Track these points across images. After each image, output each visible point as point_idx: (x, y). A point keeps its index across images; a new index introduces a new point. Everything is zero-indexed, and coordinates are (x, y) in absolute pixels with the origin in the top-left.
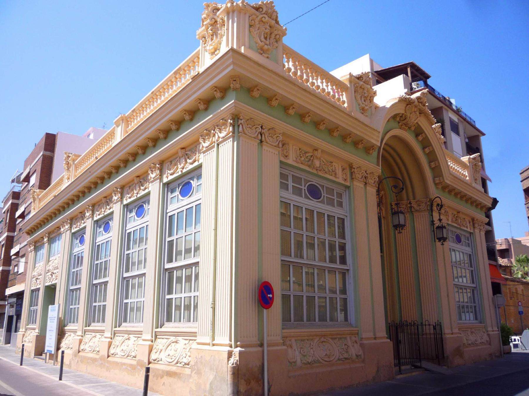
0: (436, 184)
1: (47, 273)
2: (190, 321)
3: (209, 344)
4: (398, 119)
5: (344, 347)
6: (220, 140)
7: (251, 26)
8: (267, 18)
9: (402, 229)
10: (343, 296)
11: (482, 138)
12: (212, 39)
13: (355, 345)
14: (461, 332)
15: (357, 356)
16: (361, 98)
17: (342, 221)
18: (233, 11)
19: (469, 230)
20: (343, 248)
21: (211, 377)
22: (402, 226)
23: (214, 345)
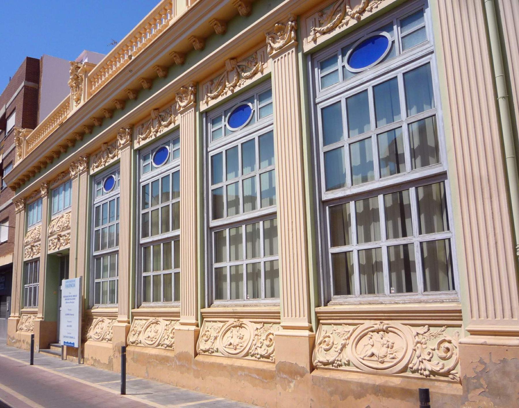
1: (49, 237)
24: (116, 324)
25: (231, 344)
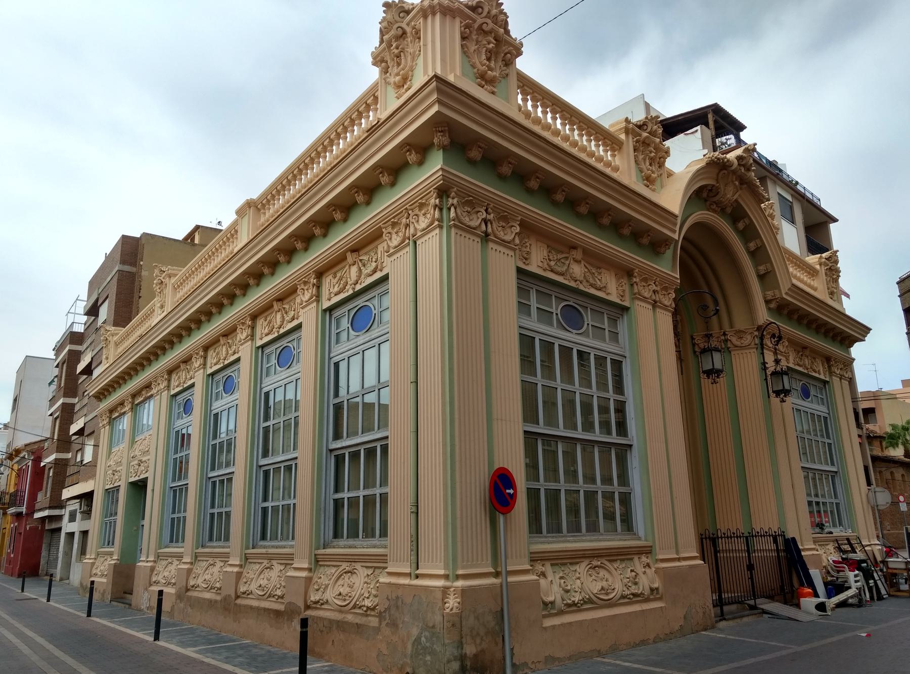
0: (767, 302)
2: (373, 536)
3: (409, 575)
4: (705, 195)
5: (629, 574)
6: (419, 234)
7: (463, 38)
8: (491, 25)
9: (718, 377)
10: (623, 489)
11: (832, 226)
12: (399, 64)
13: (648, 570)
14: (818, 547)
15: (652, 590)
16: (644, 160)
17: (617, 365)
18: (434, 14)
19: (822, 377)
20: (621, 409)
21: (415, 632)
22: (718, 372)
23: (417, 577)
24: (229, 569)
25: (340, 594)
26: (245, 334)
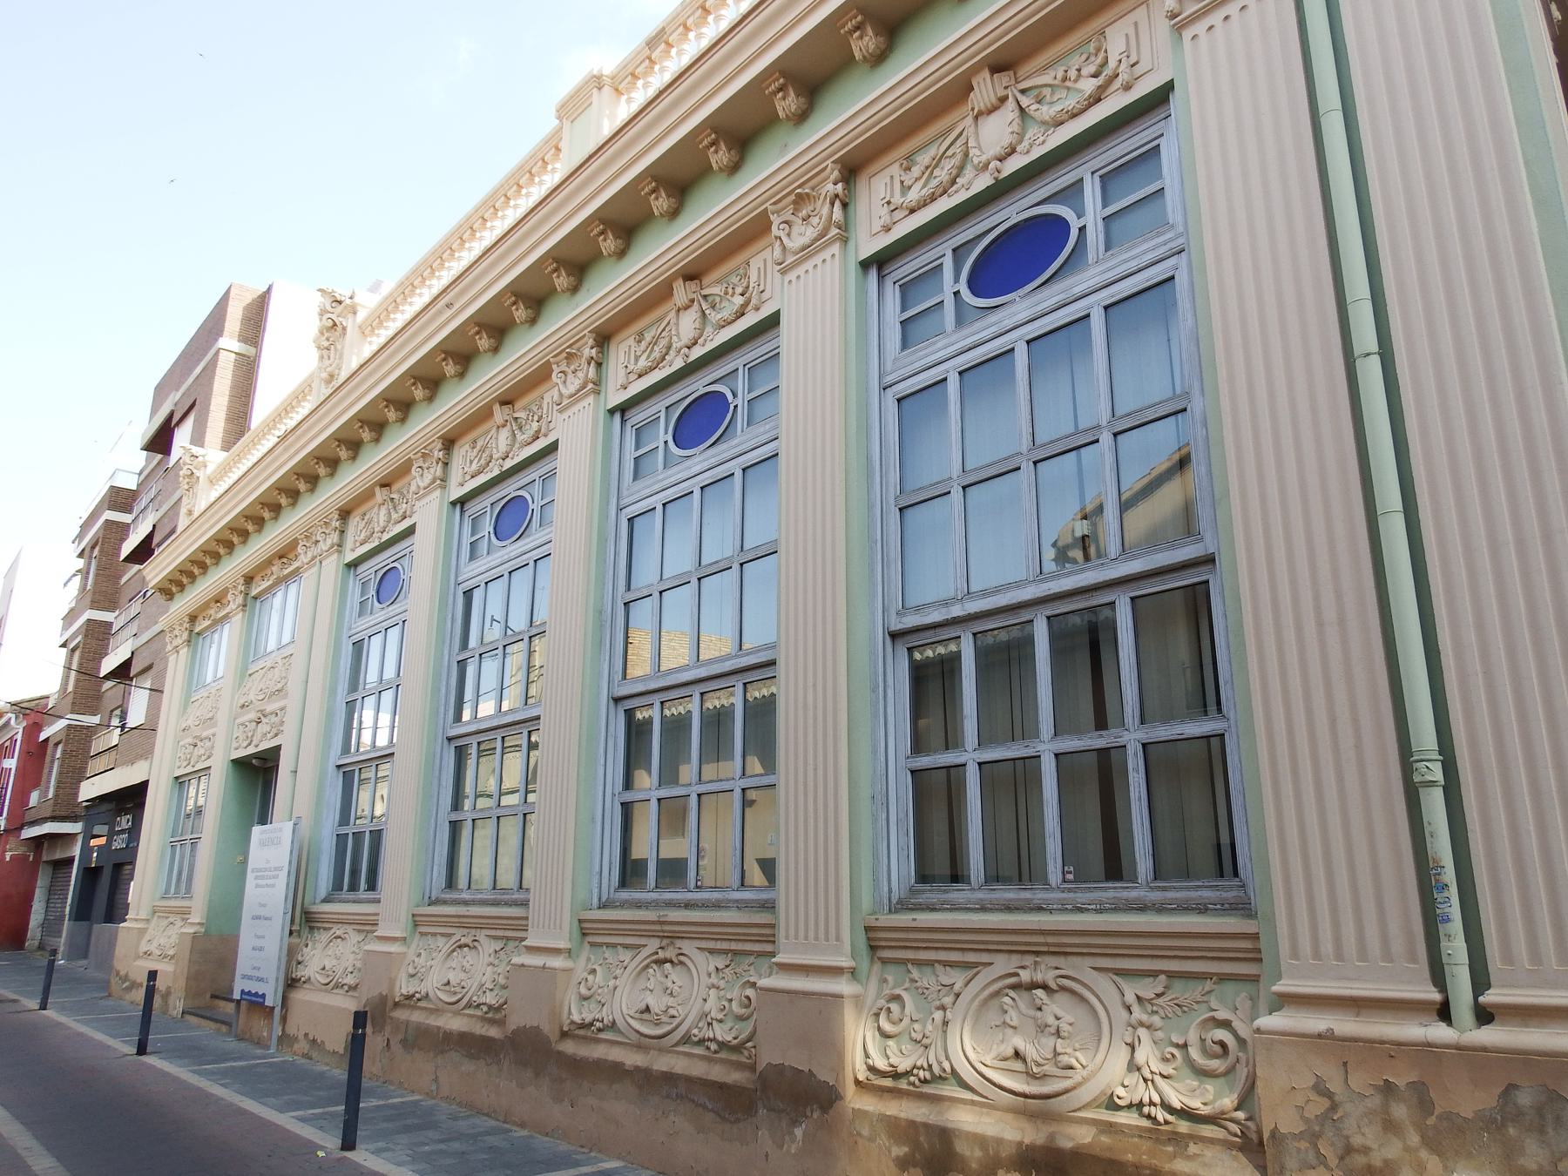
26: (428, 478)
